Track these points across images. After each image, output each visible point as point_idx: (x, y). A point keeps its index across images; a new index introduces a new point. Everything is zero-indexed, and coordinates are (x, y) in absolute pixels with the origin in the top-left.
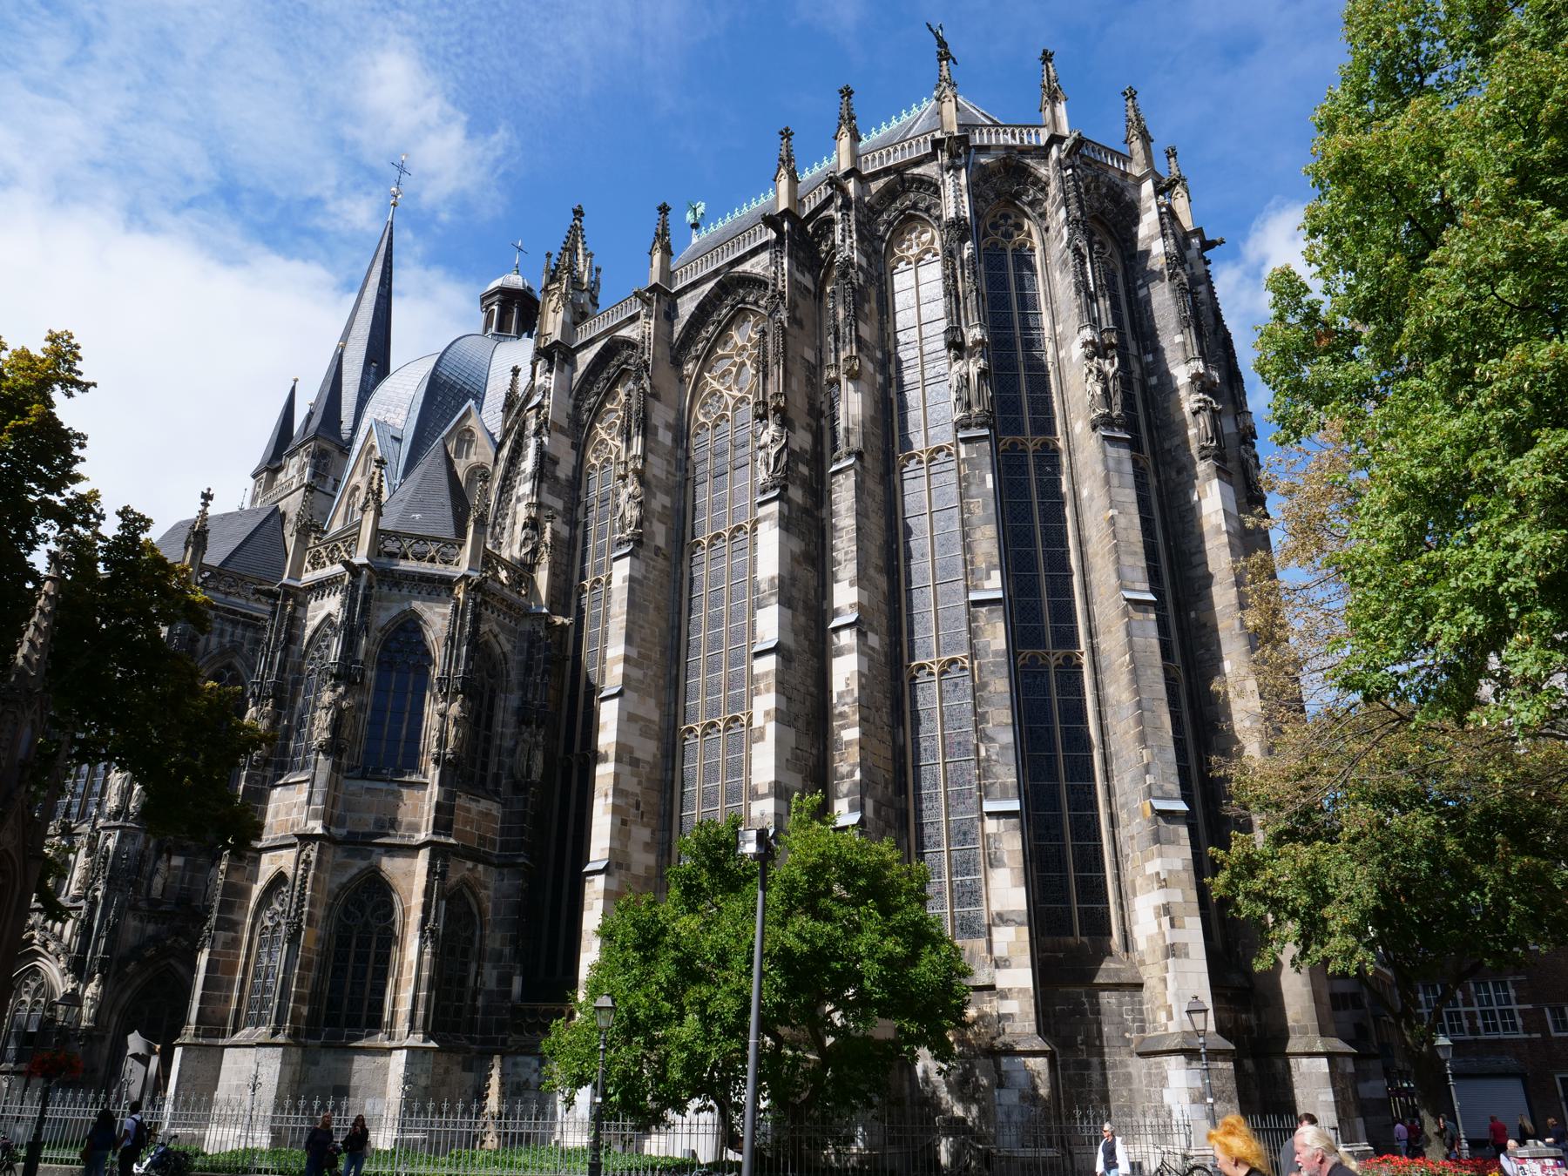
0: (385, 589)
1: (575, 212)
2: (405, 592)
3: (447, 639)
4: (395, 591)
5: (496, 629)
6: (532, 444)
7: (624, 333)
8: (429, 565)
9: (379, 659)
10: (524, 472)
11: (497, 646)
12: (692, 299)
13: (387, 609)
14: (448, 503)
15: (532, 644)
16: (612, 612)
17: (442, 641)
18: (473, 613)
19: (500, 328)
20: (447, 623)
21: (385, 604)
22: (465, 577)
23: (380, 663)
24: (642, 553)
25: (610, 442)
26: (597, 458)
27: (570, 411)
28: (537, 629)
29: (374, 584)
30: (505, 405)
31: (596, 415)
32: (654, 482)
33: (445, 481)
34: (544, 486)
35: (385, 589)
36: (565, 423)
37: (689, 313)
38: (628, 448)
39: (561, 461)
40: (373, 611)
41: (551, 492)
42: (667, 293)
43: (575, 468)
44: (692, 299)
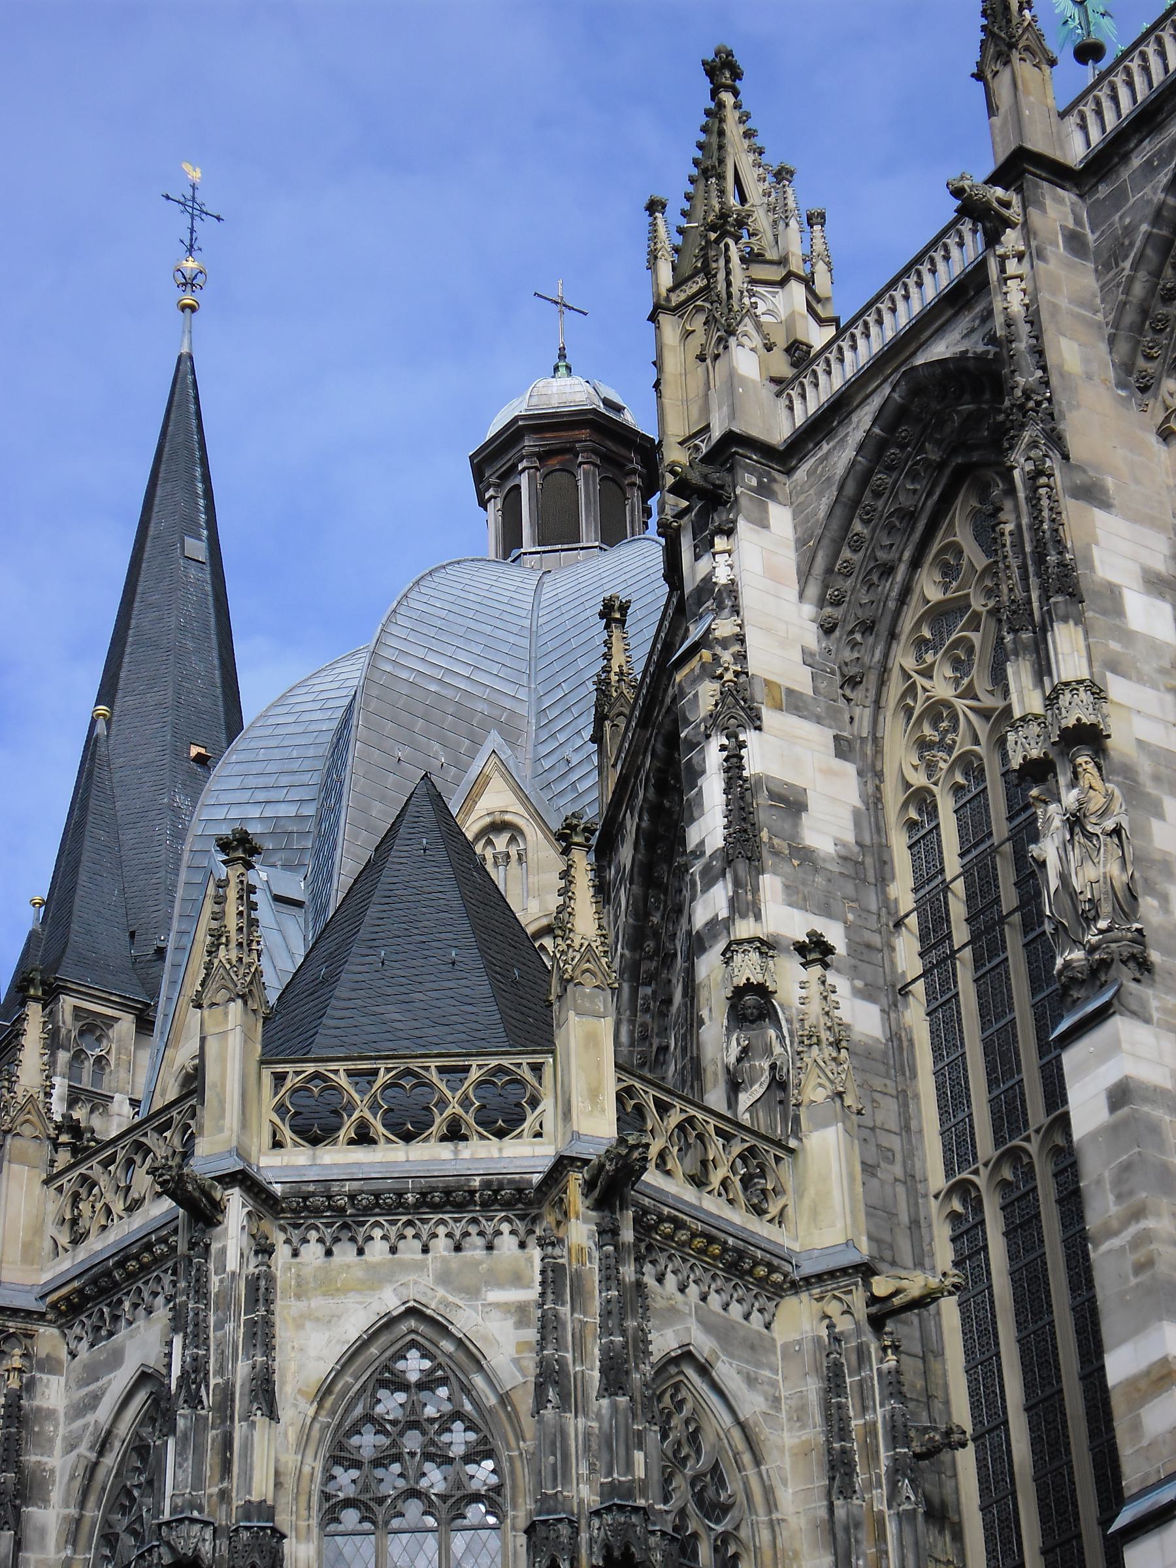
0: (312, 1252)
1: (711, 70)
2: (377, 1250)
3: (540, 1388)
4: (345, 1253)
5: (704, 1344)
6: (713, 756)
7: (941, 349)
8: (445, 1151)
9: (326, 1496)
10: (699, 852)
11: (713, 1399)
12: (1149, 168)
13: (329, 1320)
14: (470, 958)
15: (834, 1381)
16: (1093, 1221)
17: (525, 1402)
18: (609, 1276)
19: (542, 538)
20: (531, 1334)
21: (317, 1303)
22: (563, 1164)
23: (332, 1510)
24: (1153, 998)
25: (960, 705)
26: (931, 768)
27: (811, 637)
28: (844, 1325)
29: (278, 1238)
30: (600, 719)
31: (893, 636)
32: (1145, 767)
33: (452, 897)
34: (770, 885)
35: (312, 1252)
36: (801, 680)
37: (1149, 211)
38: (1043, 669)
39: (812, 800)
40: (283, 1333)
41: (796, 896)
42: (1059, 173)
43: (856, 814)
44: (1149, 168)
